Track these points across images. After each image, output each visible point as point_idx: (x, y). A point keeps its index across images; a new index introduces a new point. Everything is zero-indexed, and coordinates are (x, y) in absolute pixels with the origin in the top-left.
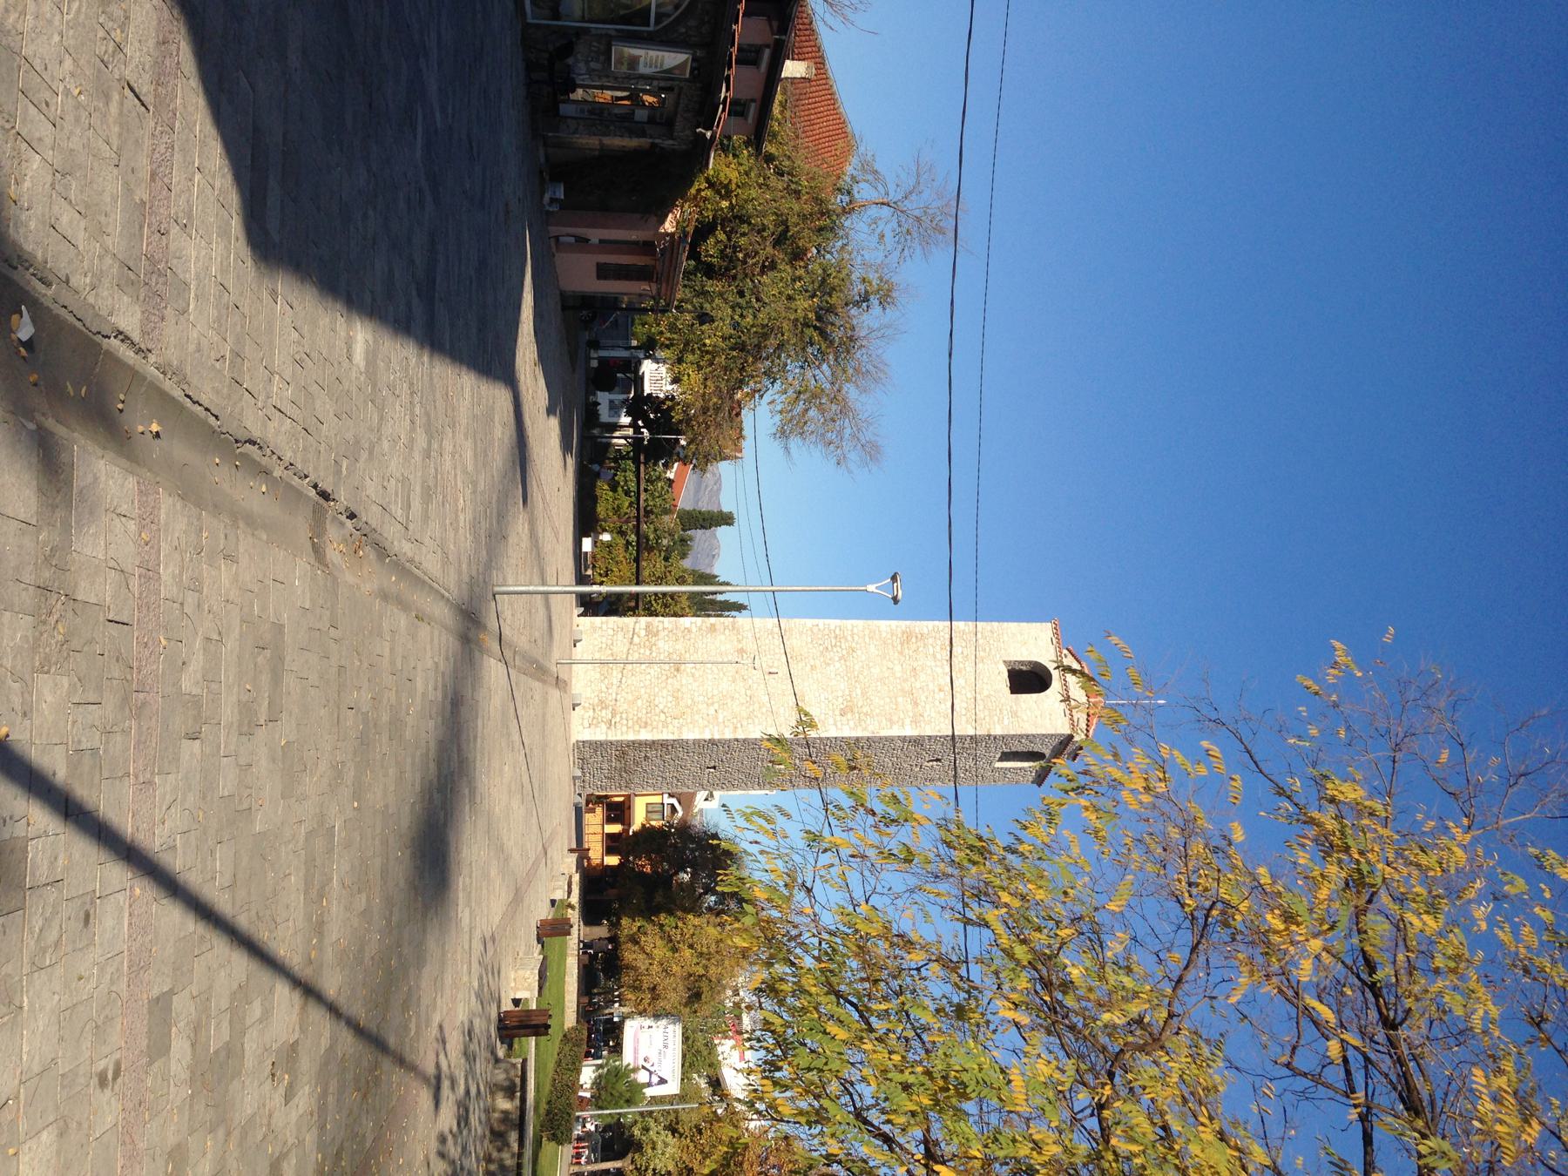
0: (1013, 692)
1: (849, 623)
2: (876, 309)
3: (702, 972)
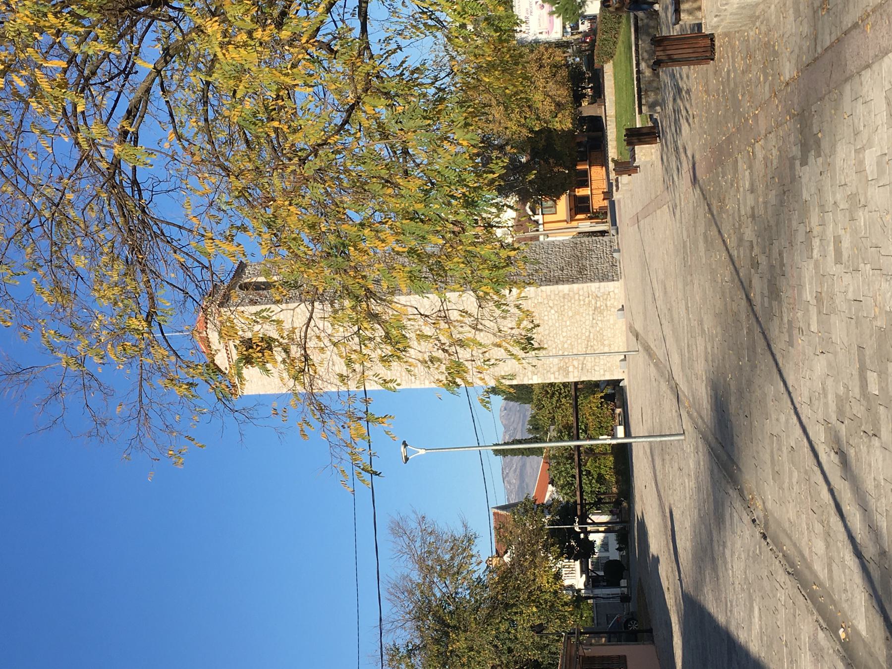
2: (400, 643)
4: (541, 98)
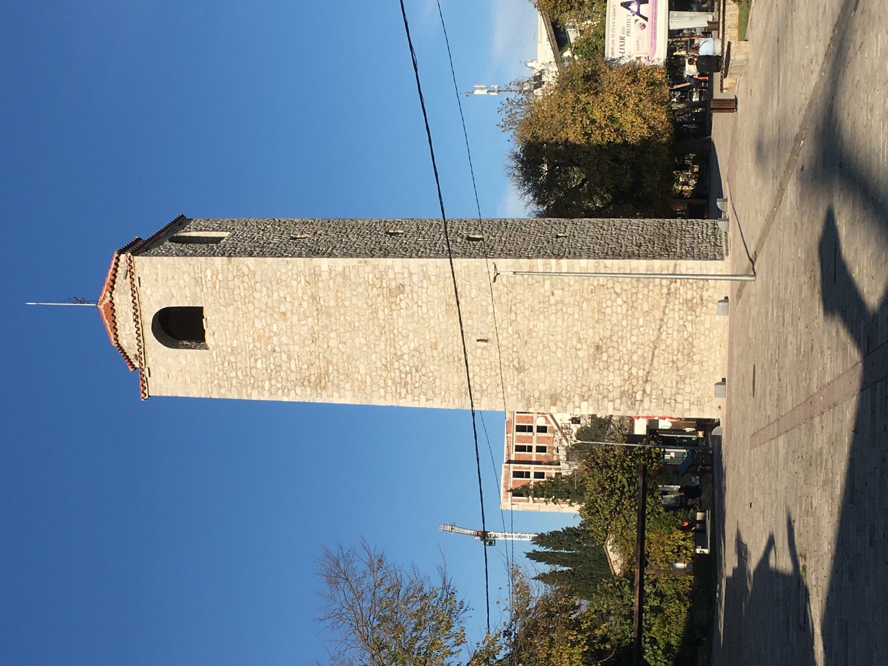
0: (200, 309)
1: (389, 402)
3: (582, 97)
4: (631, 118)
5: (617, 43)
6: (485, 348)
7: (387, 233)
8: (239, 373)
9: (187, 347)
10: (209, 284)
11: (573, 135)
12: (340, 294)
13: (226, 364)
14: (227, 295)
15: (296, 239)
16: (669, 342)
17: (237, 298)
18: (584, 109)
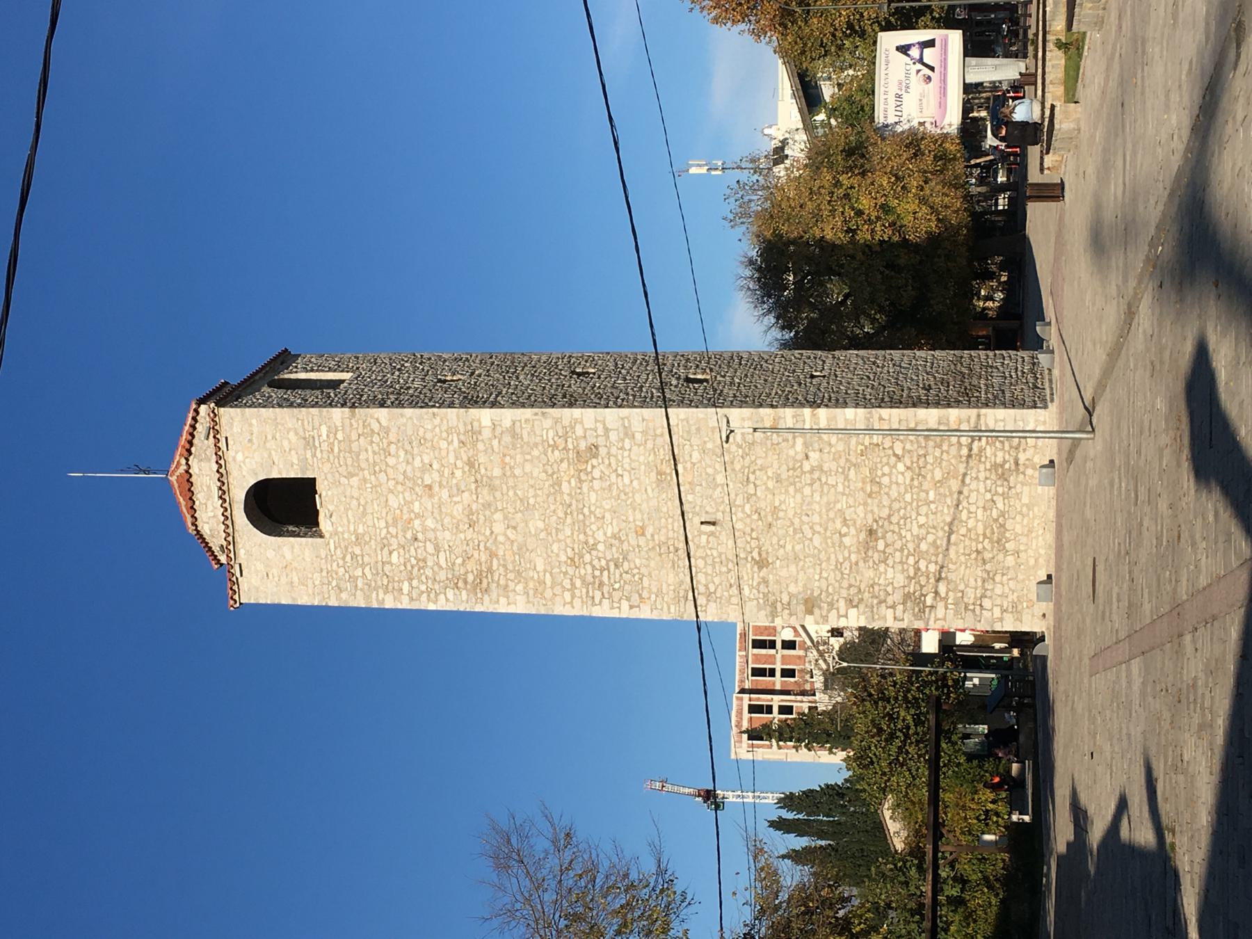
0: (312, 482)
1: (578, 610)
5: (892, 101)
6: (712, 534)
7: (573, 372)
8: (367, 570)
9: (293, 534)
10: (325, 446)
11: (831, 231)
12: (507, 459)
13: (348, 558)
14: (349, 461)
15: (445, 381)
16: (971, 523)
17: (363, 465)
18: (847, 196)
